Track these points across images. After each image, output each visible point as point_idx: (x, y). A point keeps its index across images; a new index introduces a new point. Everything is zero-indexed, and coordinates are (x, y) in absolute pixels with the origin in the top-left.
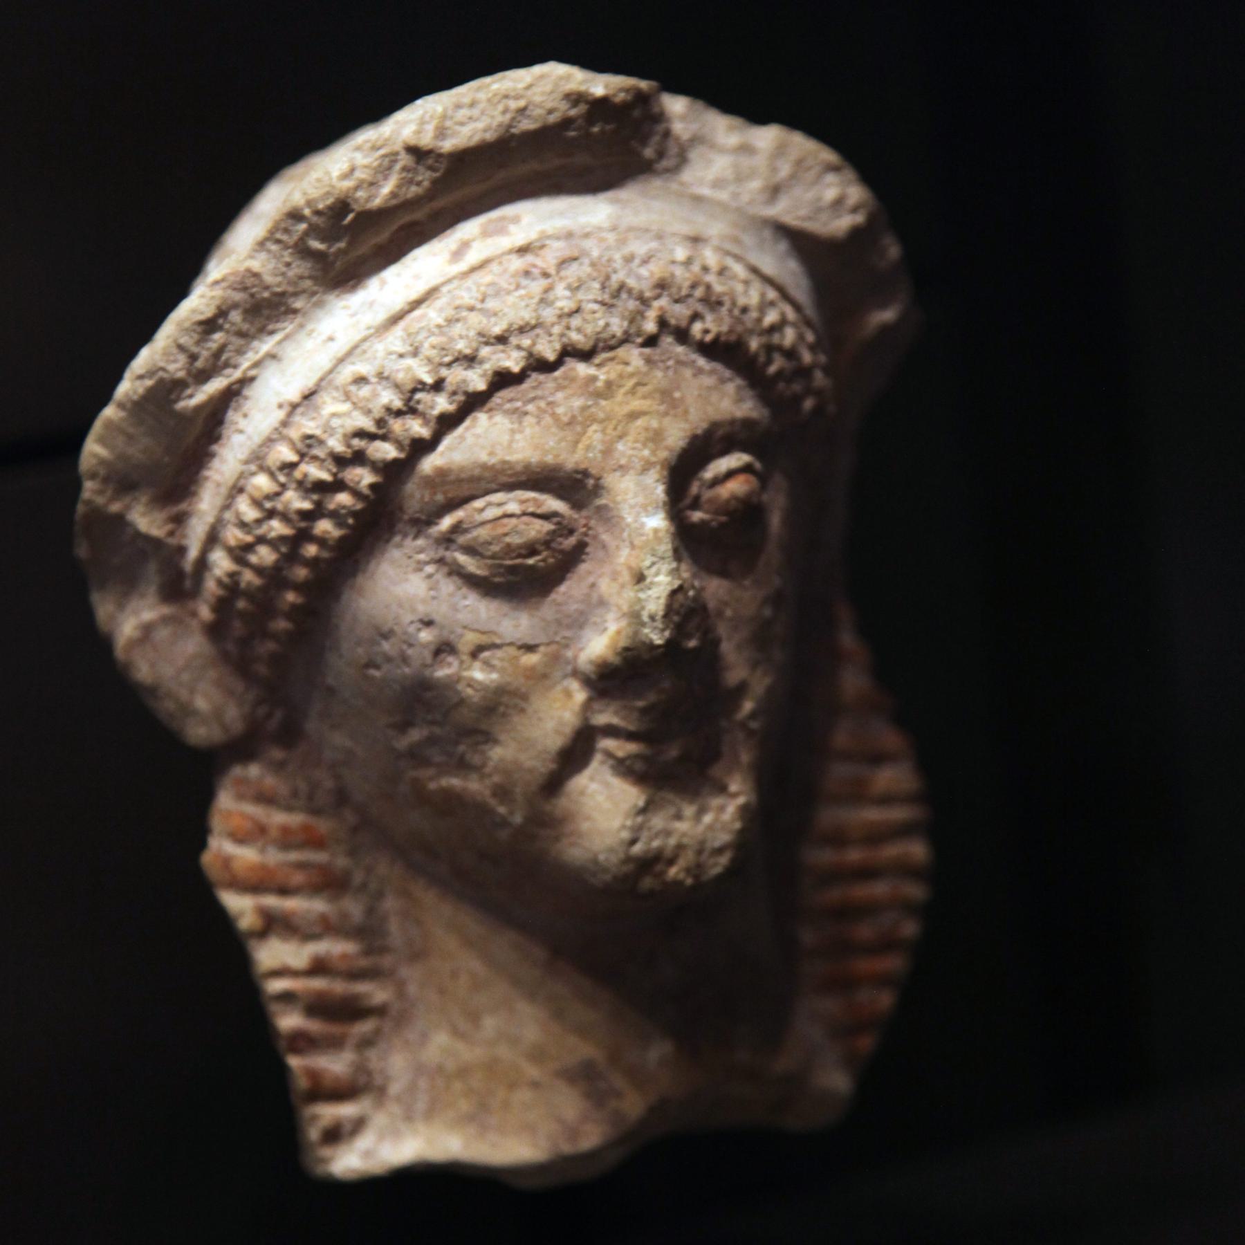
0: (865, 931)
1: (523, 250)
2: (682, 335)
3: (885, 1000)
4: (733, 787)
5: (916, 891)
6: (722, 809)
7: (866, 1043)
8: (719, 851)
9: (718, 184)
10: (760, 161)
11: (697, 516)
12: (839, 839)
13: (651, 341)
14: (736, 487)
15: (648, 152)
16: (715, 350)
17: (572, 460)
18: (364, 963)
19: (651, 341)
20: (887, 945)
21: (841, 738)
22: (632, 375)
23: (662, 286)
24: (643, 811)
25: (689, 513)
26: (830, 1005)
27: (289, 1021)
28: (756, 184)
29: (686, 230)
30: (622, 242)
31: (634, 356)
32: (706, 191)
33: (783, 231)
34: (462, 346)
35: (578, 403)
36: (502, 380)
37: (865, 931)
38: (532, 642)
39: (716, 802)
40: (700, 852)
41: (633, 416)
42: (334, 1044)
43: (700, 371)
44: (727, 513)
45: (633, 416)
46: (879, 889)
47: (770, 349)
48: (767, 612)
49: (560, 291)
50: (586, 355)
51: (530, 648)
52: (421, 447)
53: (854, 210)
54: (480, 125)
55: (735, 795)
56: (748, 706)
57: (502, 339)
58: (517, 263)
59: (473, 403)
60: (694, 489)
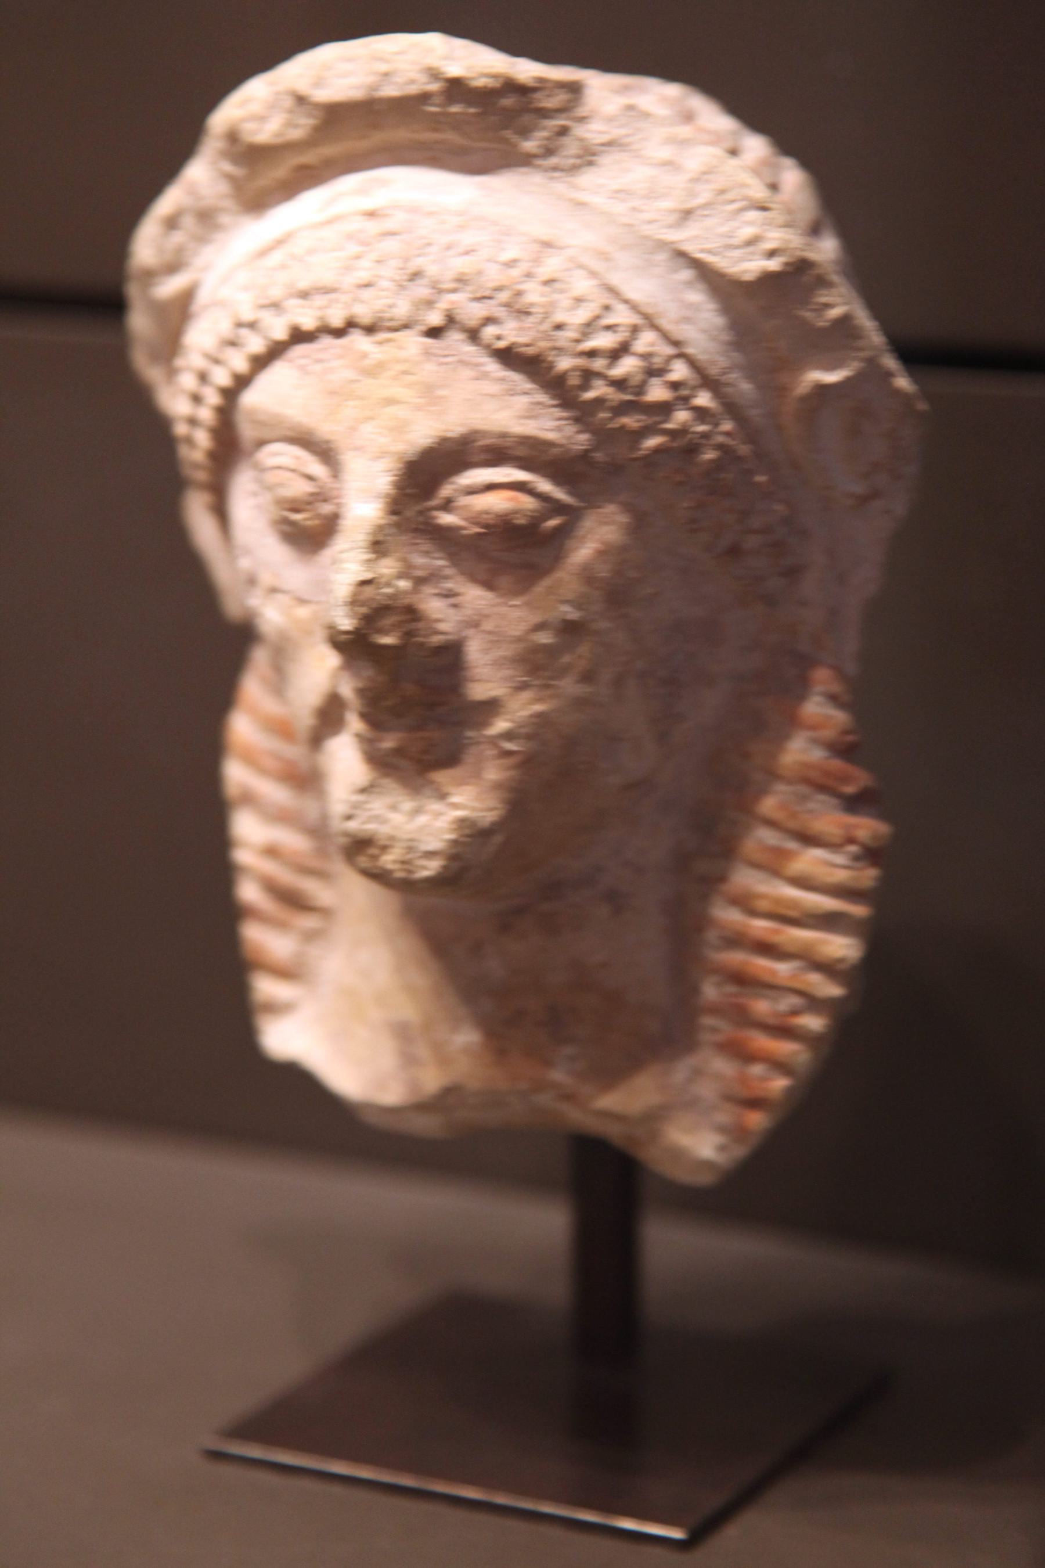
0: (762, 1007)
1: (371, 214)
2: (473, 335)
3: (780, 1084)
4: (455, 799)
5: (833, 990)
6: (438, 815)
7: (757, 1120)
8: (430, 854)
9: (622, 194)
10: (678, 181)
11: (447, 519)
12: (745, 903)
13: (434, 333)
14: (497, 502)
15: (529, 145)
16: (508, 357)
17: (325, 429)
18: (314, 863)
19: (434, 333)
20: (784, 1031)
21: (769, 805)
22: (406, 361)
23: (461, 281)
24: (363, 791)
25: (436, 513)
26: (723, 1066)
27: (249, 892)
28: (667, 204)
29: (544, 232)
30: (461, 228)
31: (413, 342)
32: (597, 200)
33: (681, 255)
34: (276, 293)
35: (349, 374)
36: (299, 336)
37: (762, 1007)
38: (306, 597)
39: (436, 806)
40: (410, 849)
41: (390, 401)
42: (281, 925)
43: (485, 376)
44: (486, 526)
45: (390, 401)
46: (783, 969)
47: (588, 376)
48: (545, 638)
49: (365, 263)
50: (370, 329)
51: (302, 601)
52: (242, 382)
53: (772, 254)
54: (353, 81)
55: (455, 806)
56: (501, 725)
57: (304, 295)
58: (358, 224)
59: (275, 352)
60: (446, 491)
